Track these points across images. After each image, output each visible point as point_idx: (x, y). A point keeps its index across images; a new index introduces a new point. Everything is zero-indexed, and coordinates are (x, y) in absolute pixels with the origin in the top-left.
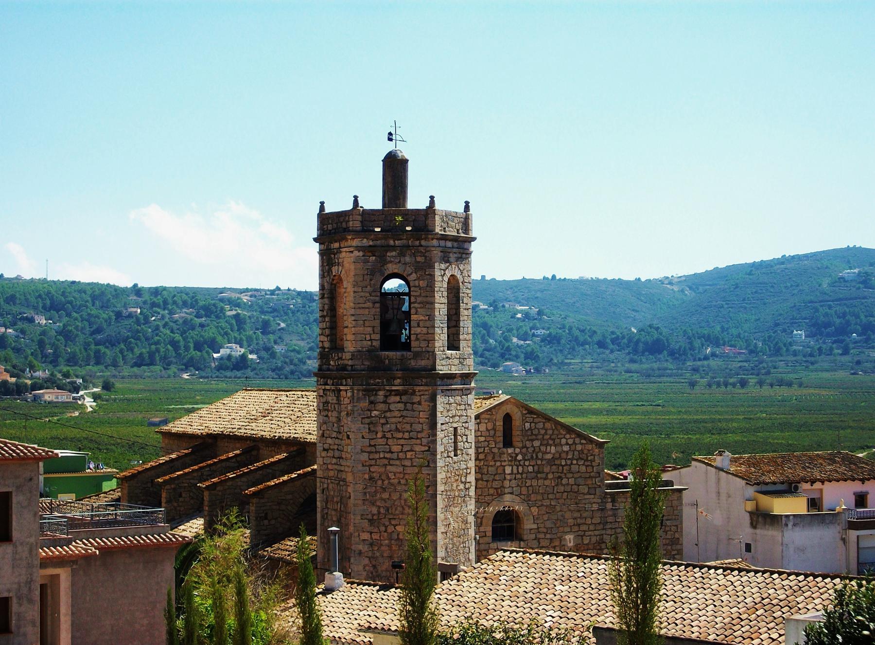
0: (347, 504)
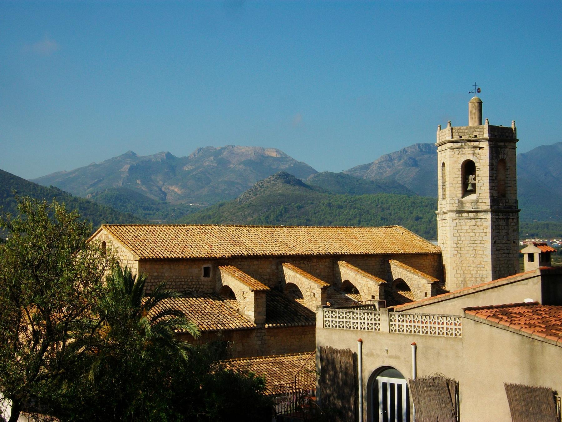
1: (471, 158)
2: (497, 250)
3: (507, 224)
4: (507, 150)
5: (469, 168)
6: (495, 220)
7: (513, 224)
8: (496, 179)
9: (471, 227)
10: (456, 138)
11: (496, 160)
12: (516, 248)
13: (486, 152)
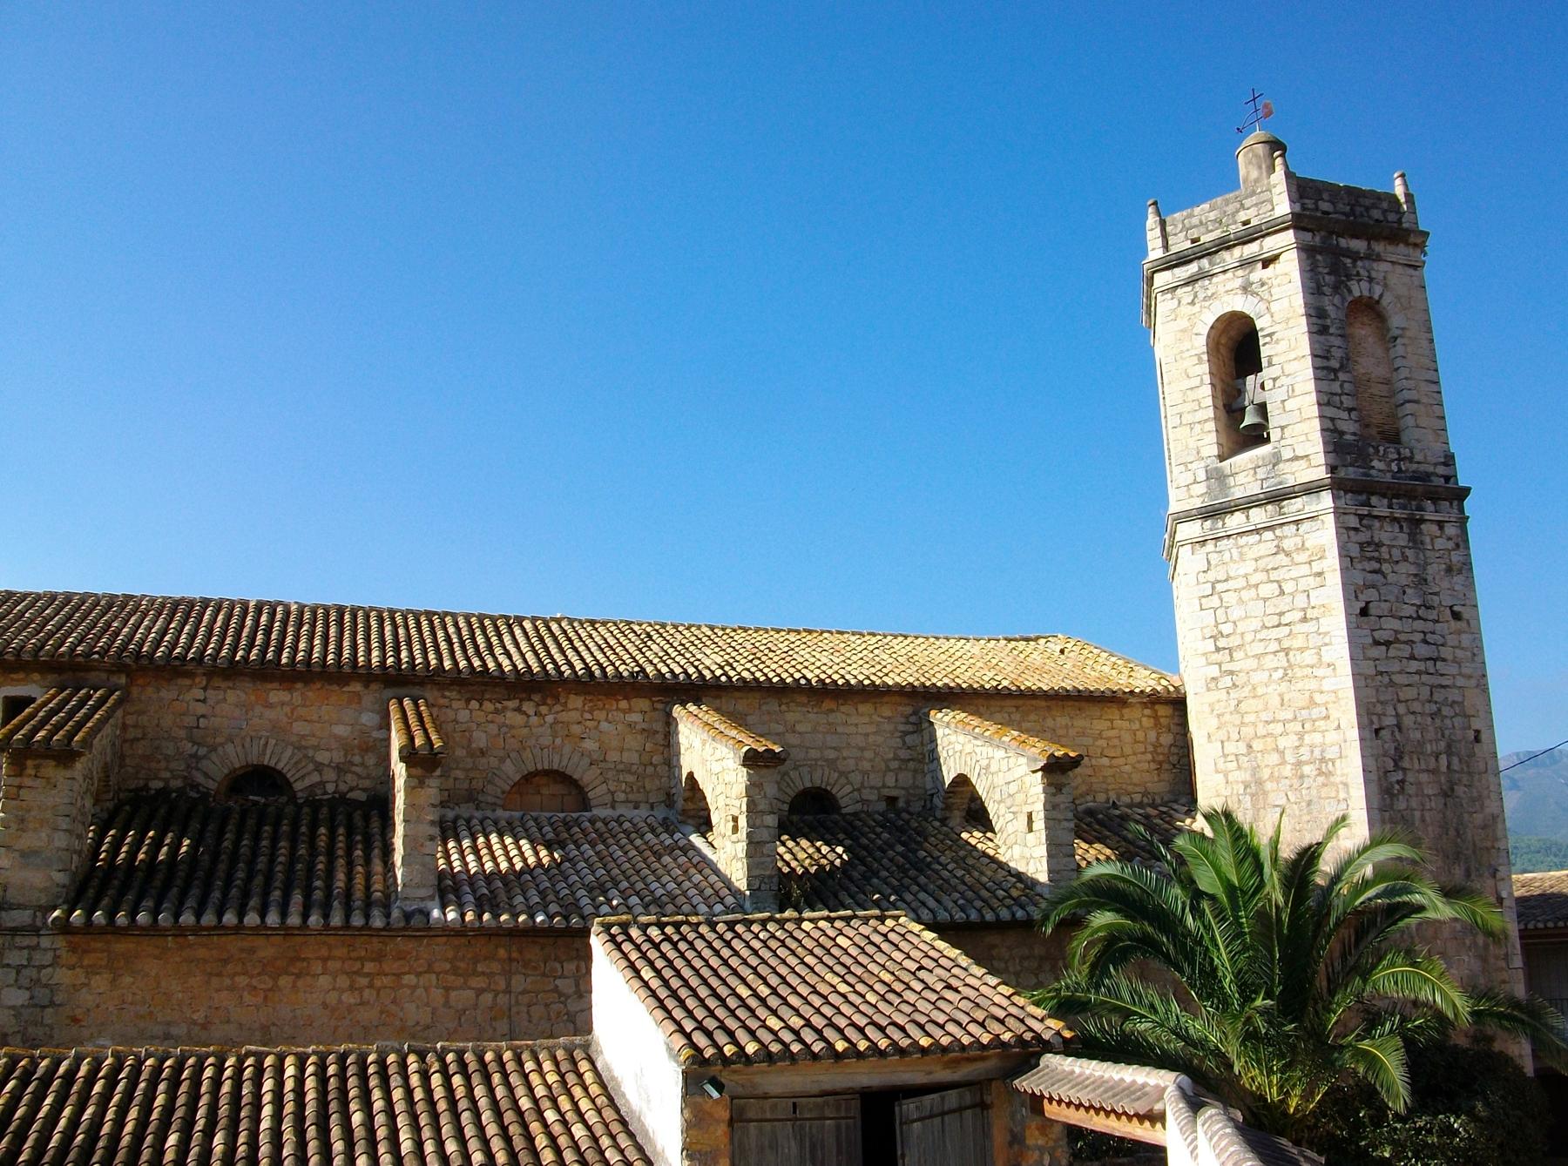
0: (1472, 755)
1: (1240, 304)
2: (1377, 643)
3: (1415, 540)
4: (1383, 267)
5: (1238, 348)
6: (1353, 521)
7: (1440, 543)
8: (1342, 367)
9: (1262, 564)
10: (1180, 244)
11: (1337, 300)
12: (1466, 639)
13: (1289, 269)
